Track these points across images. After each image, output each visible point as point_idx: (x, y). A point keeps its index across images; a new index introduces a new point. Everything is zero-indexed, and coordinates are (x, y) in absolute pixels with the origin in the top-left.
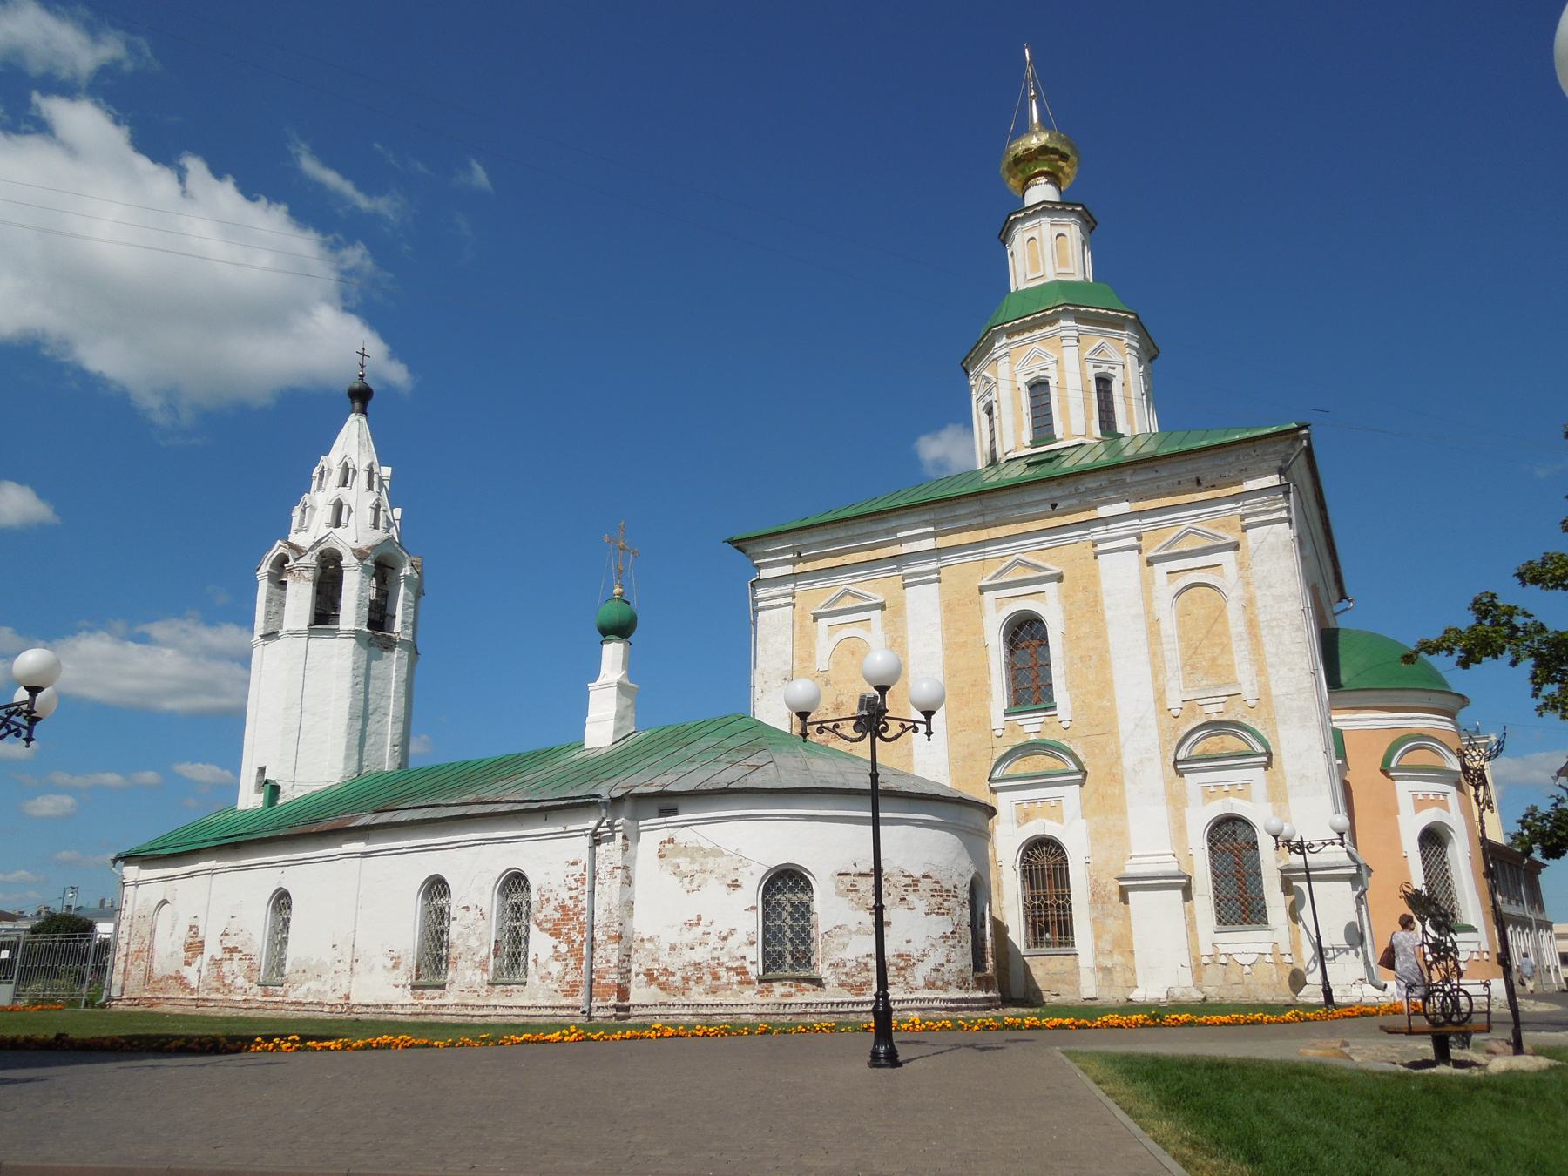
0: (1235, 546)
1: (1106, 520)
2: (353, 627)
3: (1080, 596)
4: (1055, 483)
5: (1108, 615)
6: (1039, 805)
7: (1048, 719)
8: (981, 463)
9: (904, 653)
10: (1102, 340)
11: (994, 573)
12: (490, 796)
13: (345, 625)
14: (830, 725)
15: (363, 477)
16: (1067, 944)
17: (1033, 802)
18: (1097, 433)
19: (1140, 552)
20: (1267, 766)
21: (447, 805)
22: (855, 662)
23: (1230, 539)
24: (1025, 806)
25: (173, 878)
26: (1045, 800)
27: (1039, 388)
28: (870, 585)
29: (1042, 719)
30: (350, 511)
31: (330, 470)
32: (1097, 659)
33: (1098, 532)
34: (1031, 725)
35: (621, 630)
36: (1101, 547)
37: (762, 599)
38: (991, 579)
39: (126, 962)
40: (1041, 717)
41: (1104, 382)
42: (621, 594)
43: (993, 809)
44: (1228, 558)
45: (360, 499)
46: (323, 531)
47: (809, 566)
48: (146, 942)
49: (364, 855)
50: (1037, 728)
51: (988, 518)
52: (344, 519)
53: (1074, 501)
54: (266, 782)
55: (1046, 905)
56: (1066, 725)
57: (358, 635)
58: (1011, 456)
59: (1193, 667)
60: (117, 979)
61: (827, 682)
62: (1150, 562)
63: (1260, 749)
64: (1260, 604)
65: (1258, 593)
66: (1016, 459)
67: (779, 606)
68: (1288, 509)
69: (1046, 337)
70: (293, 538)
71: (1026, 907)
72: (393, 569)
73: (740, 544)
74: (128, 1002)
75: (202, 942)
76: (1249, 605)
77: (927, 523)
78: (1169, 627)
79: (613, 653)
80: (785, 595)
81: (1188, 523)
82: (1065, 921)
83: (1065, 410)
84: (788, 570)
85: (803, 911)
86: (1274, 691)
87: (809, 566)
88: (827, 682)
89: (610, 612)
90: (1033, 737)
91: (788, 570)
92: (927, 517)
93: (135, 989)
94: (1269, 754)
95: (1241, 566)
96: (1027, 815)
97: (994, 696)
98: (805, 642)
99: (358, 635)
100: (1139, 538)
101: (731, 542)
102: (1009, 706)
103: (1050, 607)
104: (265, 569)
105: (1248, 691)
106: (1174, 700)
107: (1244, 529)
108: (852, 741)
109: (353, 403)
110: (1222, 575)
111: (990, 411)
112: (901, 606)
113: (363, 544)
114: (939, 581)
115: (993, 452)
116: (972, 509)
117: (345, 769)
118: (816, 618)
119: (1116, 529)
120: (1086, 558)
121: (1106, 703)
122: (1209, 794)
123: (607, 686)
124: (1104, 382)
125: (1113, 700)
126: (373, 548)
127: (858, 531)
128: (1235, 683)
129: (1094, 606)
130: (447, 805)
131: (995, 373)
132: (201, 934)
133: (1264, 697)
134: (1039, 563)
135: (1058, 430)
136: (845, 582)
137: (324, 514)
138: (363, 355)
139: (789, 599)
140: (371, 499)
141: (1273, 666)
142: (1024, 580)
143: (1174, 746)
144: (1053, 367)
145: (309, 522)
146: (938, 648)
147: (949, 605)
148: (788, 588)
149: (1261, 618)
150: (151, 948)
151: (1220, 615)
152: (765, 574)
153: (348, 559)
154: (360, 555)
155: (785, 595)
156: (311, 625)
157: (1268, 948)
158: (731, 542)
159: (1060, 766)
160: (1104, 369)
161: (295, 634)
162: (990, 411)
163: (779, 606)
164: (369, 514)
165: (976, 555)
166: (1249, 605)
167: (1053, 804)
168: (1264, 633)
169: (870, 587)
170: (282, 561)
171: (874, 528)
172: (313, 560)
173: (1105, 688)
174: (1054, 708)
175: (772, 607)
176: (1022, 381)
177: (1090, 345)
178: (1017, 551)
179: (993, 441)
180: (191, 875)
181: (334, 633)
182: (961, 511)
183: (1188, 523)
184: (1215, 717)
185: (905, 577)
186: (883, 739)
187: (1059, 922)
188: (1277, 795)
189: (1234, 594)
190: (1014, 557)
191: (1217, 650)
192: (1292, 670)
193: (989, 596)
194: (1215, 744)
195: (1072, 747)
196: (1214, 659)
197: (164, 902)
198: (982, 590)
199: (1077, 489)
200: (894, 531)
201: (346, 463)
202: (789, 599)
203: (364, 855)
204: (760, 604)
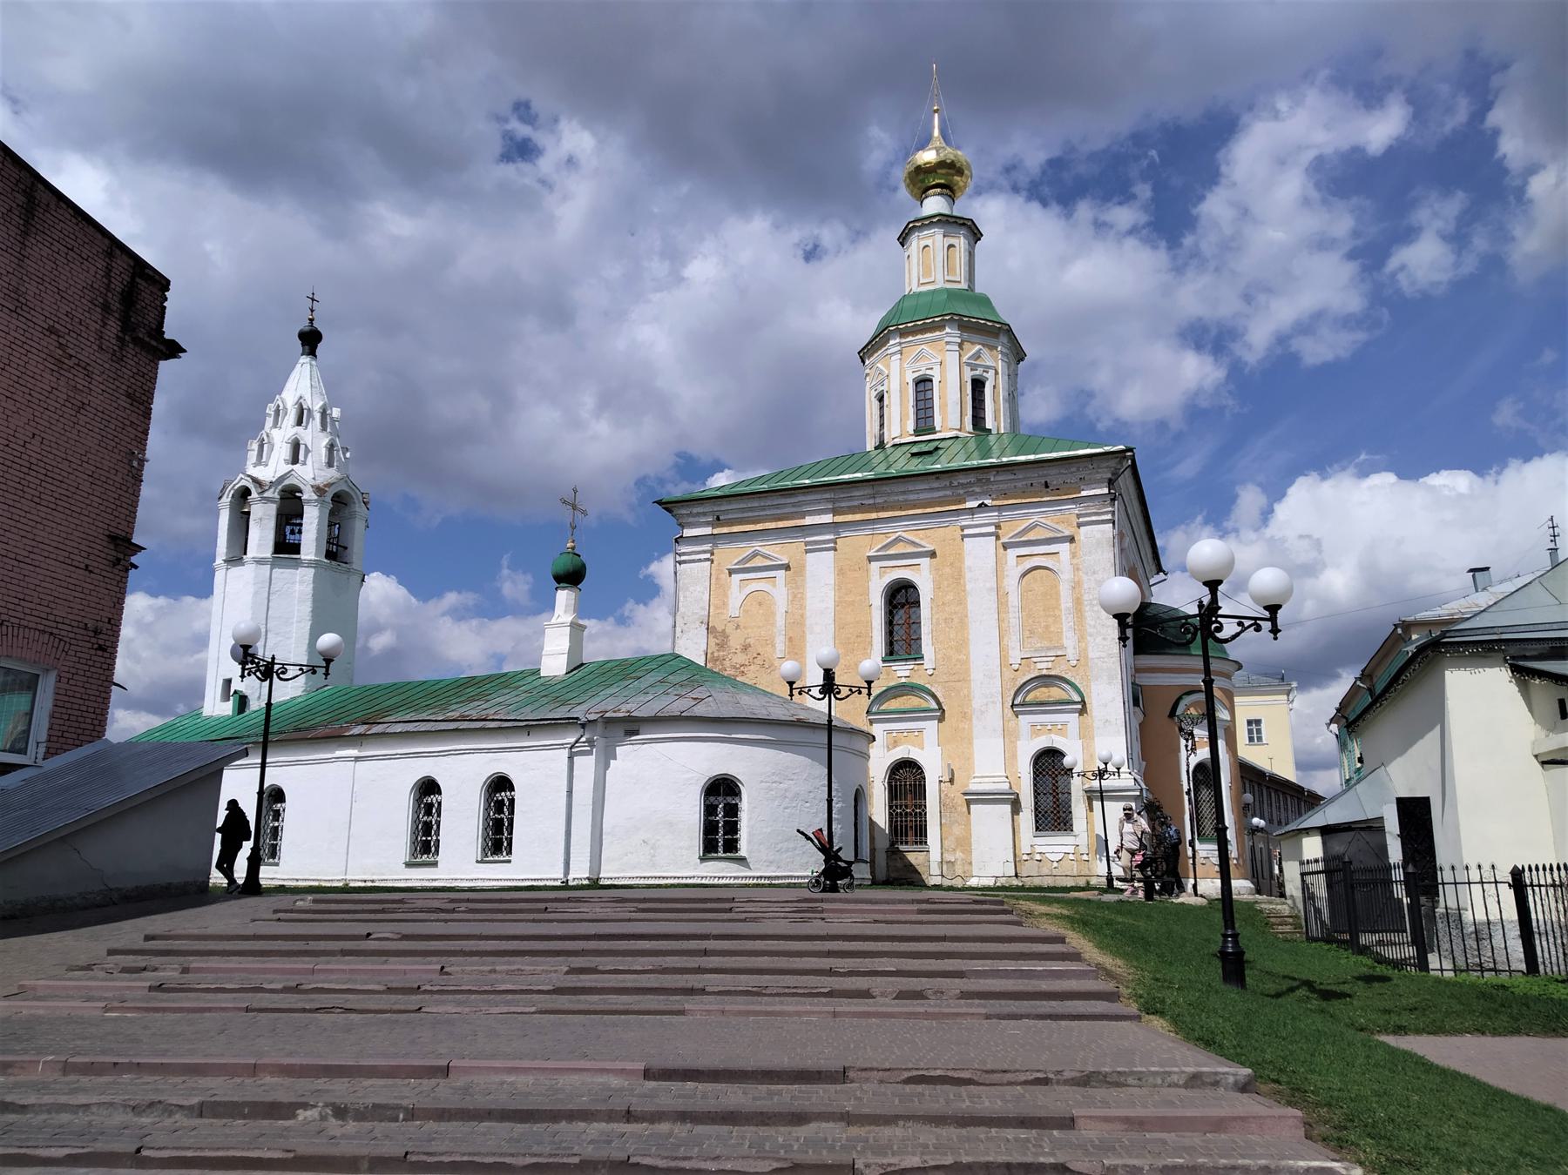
0: (1072, 540)
1: (971, 511)
2: (313, 558)
3: (948, 570)
4: (934, 477)
5: (969, 587)
6: (905, 734)
7: (916, 667)
8: (870, 446)
9: (803, 607)
10: (978, 347)
11: (880, 546)
12: (474, 714)
13: (308, 554)
14: (806, 690)
15: (318, 416)
16: (921, 843)
17: (900, 731)
18: (969, 427)
19: (998, 538)
20: (1083, 711)
21: (436, 721)
22: (761, 611)
23: (1067, 533)
24: (894, 735)
26: (910, 731)
27: (923, 383)
28: (778, 548)
29: (911, 667)
30: (307, 451)
31: (285, 409)
32: (958, 621)
33: (966, 521)
34: (902, 672)
35: (572, 577)
36: (967, 532)
37: (684, 554)
38: (878, 551)
40: (910, 665)
41: (978, 385)
42: (573, 548)
43: (874, 737)
44: (1064, 548)
45: (315, 439)
46: (284, 468)
47: (725, 530)
49: (357, 759)
50: (907, 673)
51: (879, 500)
52: (301, 457)
53: (948, 493)
54: (236, 692)
55: (906, 813)
56: (930, 672)
58: (897, 441)
59: (1031, 632)
61: (738, 627)
62: (1005, 547)
63: (1077, 698)
64: (1086, 586)
65: (1085, 578)
66: (901, 445)
68: (1113, 513)
69: (933, 341)
70: (252, 471)
71: (890, 814)
73: (668, 506)
76: (1076, 585)
78: (1014, 600)
79: (564, 597)
80: (705, 552)
81: (1035, 518)
82: (921, 826)
83: (943, 407)
84: (708, 531)
85: (733, 811)
86: (1091, 655)
87: (725, 530)
88: (738, 627)
89: (564, 564)
90: (903, 680)
91: (708, 531)
92: (827, 496)
94: (1083, 702)
95: (1074, 555)
96: (895, 742)
97: (874, 647)
98: (717, 590)
100: (998, 527)
101: (660, 503)
102: (886, 655)
103: (923, 577)
104: (227, 499)
105: (1071, 654)
106: (1015, 656)
107: (1079, 525)
108: (819, 699)
109: (303, 345)
110: (1059, 561)
111: (881, 399)
112: (803, 567)
113: (320, 482)
114: (835, 550)
115: (882, 436)
116: (866, 492)
117: (306, 683)
118: (731, 572)
119: (980, 518)
120: (954, 540)
121: (962, 657)
122: (1036, 730)
123: (562, 625)
124: (978, 385)
125: (968, 655)
127: (769, 503)
128: (1062, 647)
129: (958, 577)
130: (436, 721)
131: (888, 367)
133: (1082, 659)
134: (917, 541)
135: (938, 424)
136: (757, 545)
137: (282, 451)
138: (313, 300)
139: (708, 556)
140: (325, 441)
141: (1091, 636)
142: (904, 554)
143: (1013, 694)
144: (937, 368)
145: (269, 457)
146: (831, 604)
147: (842, 569)
148: (707, 547)
149: (1086, 597)
151: (1055, 587)
152: (688, 532)
153: (308, 494)
154: (319, 490)
155: (705, 552)
157: (1071, 849)
158: (660, 503)
159: (924, 705)
160: (978, 372)
161: (260, 562)
162: (881, 399)
164: (324, 452)
166: (1076, 585)
167: (916, 734)
168: (1087, 609)
169: (777, 551)
170: (244, 493)
171: (783, 501)
172: (277, 496)
173: (963, 645)
174: (922, 658)
176: (910, 377)
177: (970, 350)
178: (899, 530)
179: (882, 425)
181: (298, 564)
183: (1035, 518)
184: (1045, 672)
185: (807, 544)
186: (837, 699)
187: (916, 826)
188: (1086, 735)
189: (1066, 575)
190: (897, 534)
191: (1051, 620)
192: (1104, 639)
194: (1041, 694)
195: (933, 690)
196: (1047, 627)
198: (870, 559)
199: (951, 483)
201: (301, 405)
202: (708, 556)
203: (357, 759)
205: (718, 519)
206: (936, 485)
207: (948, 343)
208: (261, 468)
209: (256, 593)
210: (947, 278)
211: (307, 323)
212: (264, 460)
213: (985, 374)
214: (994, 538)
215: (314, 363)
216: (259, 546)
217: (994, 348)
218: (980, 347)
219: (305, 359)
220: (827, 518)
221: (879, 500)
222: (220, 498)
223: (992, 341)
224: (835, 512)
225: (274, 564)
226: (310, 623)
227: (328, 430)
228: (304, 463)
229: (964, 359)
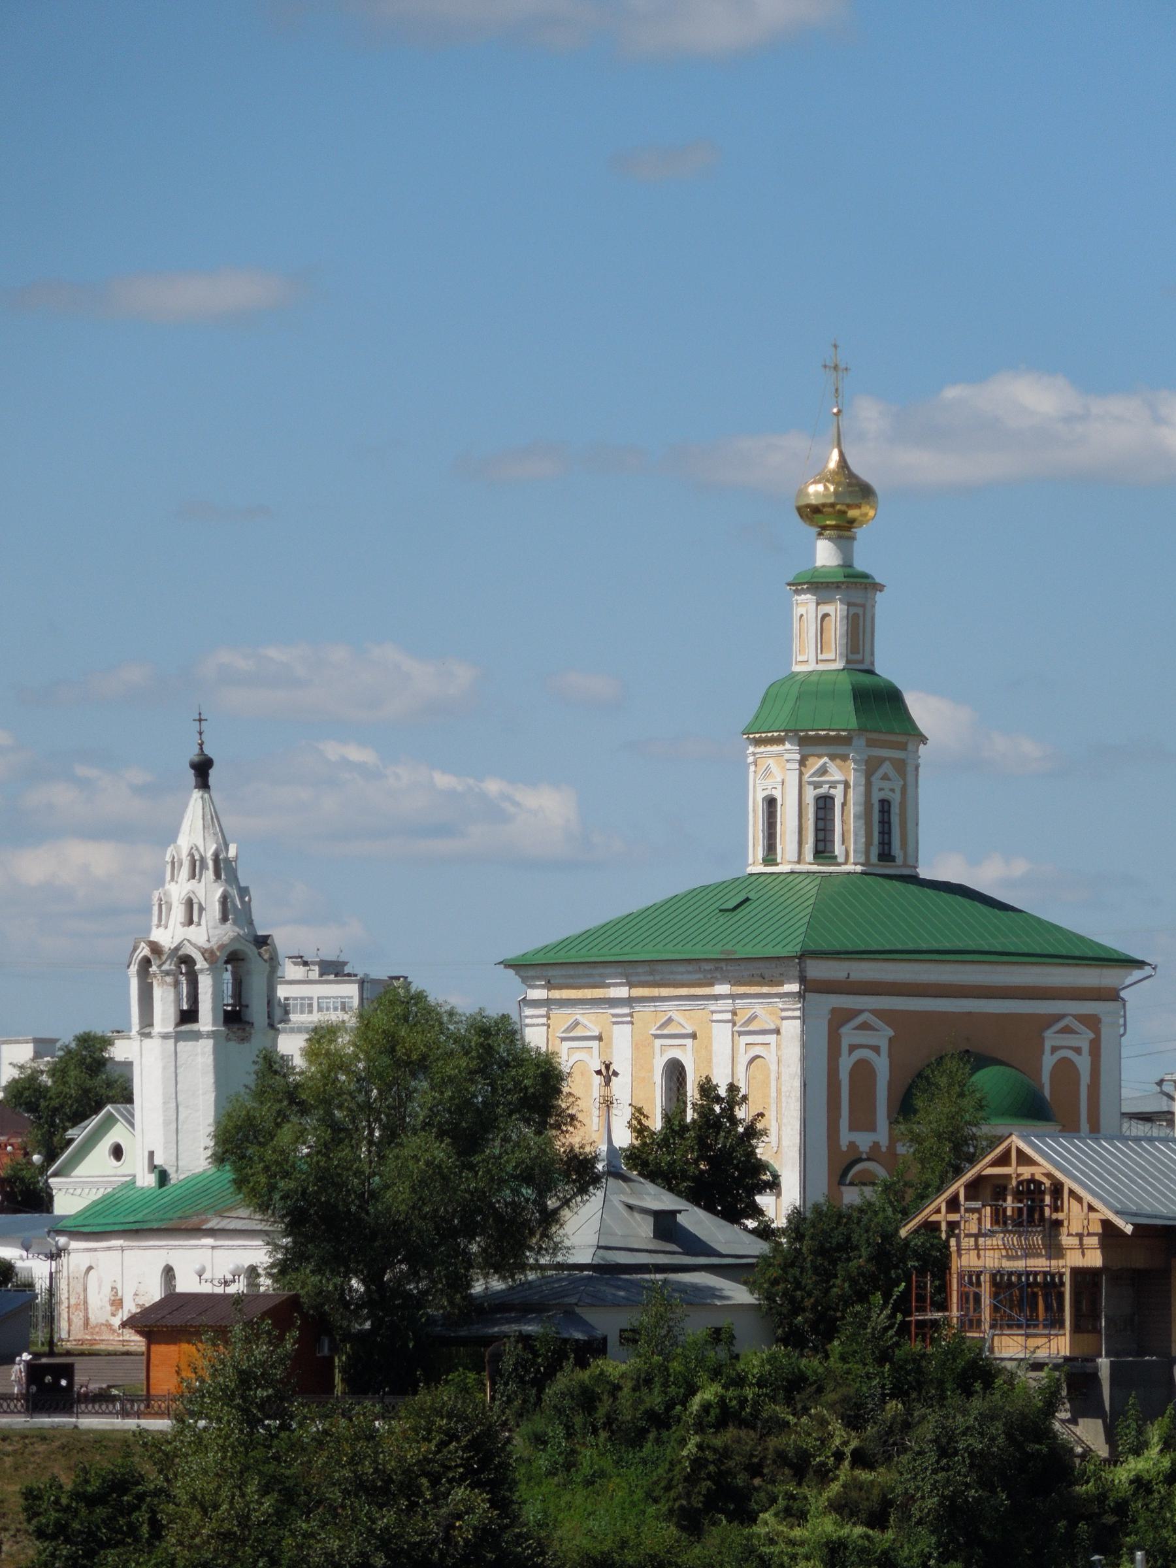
0: (777, 1032)
1: (716, 997)
13: (204, 1026)
15: (211, 864)
19: (734, 1024)
25: (95, 1250)
28: (593, 1017)
30: (201, 909)
37: (527, 1017)
39: (68, 1312)
41: (824, 804)
48: (82, 1297)
51: (657, 978)
52: (195, 919)
54: (155, 1167)
57: (213, 1035)
60: (64, 1324)
62: (740, 1033)
67: (538, 1025)
72: (243, 960)
74: (74, 1343)
75: (121, 1300)
77: (620, 975)
92: (619, 970)
93: (78, 1333)
99: (213, 1035)
100: (734, 1013)
104: (134, 969)
114: (632, 1023)
124: (824, 804)
126: (222, 947)
132: (120, 1294)
136: (578, 1014)
138: (200, 720)
148: (543, 1011)
150: (85, 1302)
154: (209, 955)
156: (178, 1025)
160: (821, 791)
161: (165, 1037)
163: (538, 1025)
165: (649, 1008)
175: (533, 1025)
180: (109, 1249)
181: (197, 1036)
182: (640, 970)
185: (614, 1016)
193: (658, 1042)
197: (90, 1268)
200: (602, 976)
203: (213, 1247)
204: (528, 1021)
205: (549, 982)
206: (690, 968)
207: (788, 761)
208: (162, 929)
209: (164, 1068)
210: (820, 657)
211: (197, 750)
212: (163, 923)
213: (832, 791)
214: (730, 1024)
215: (206, 796)
216: (163, 1020)
217: (844, 758)
218: (825, 759)
219: (197, 794)
220: (623, 992)
221: (657, 978)
222: (129, 967)
223: (841, 750)
224: (631, 985)
225: (179, 1037)
226: (213, 1095)
227: (223, 877)
228: (199, 924)
229: (806, 777)
